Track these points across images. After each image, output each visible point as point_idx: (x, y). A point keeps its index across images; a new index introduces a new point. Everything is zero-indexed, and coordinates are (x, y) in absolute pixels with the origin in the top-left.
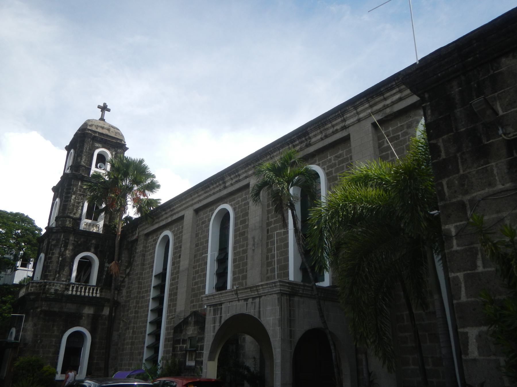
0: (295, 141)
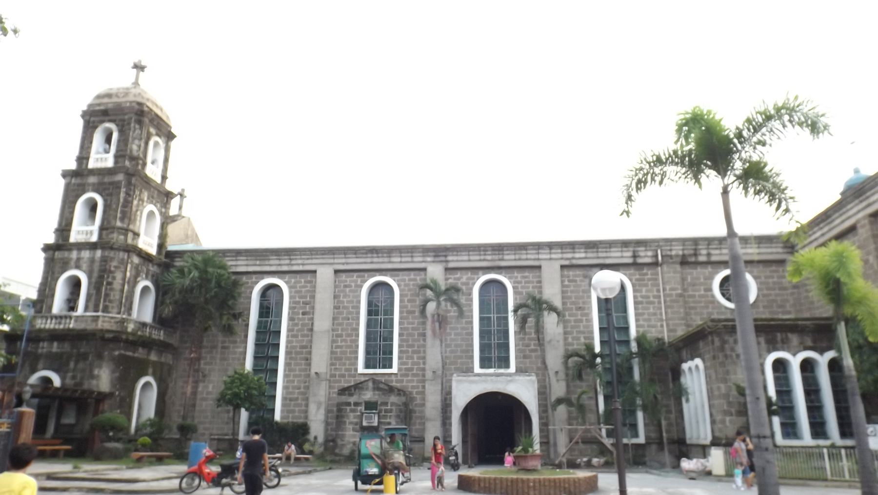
0: (487, 251)
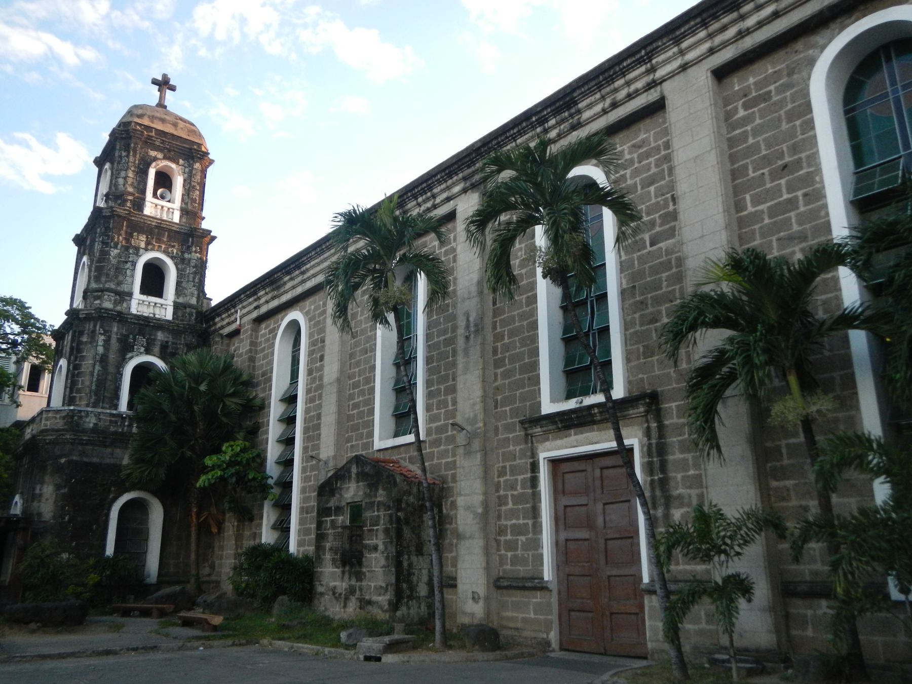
0: (547, 121)
